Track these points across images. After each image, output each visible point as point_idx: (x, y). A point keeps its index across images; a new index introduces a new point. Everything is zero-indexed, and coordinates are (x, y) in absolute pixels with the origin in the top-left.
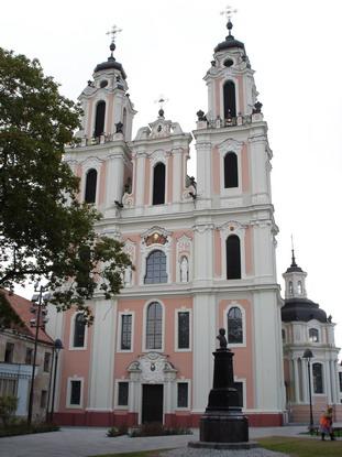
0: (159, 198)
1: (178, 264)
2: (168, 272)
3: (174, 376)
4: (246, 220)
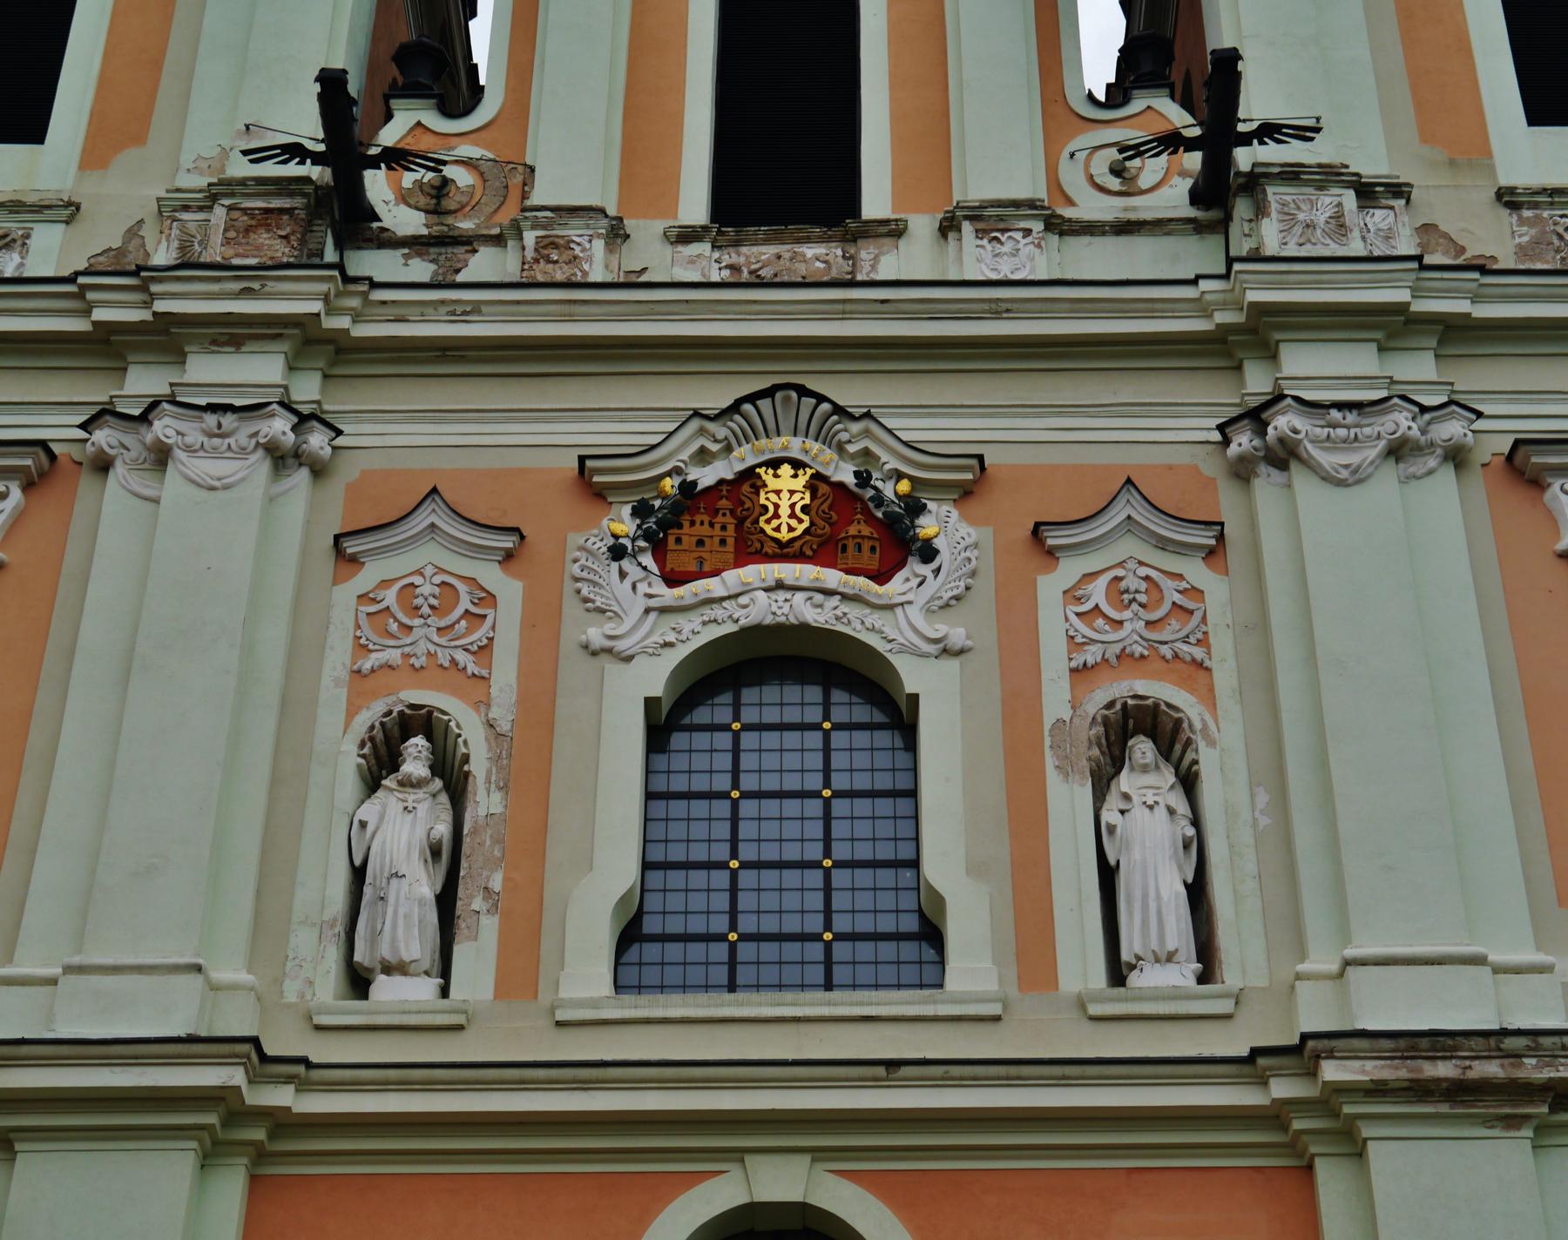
2: (945, 863)
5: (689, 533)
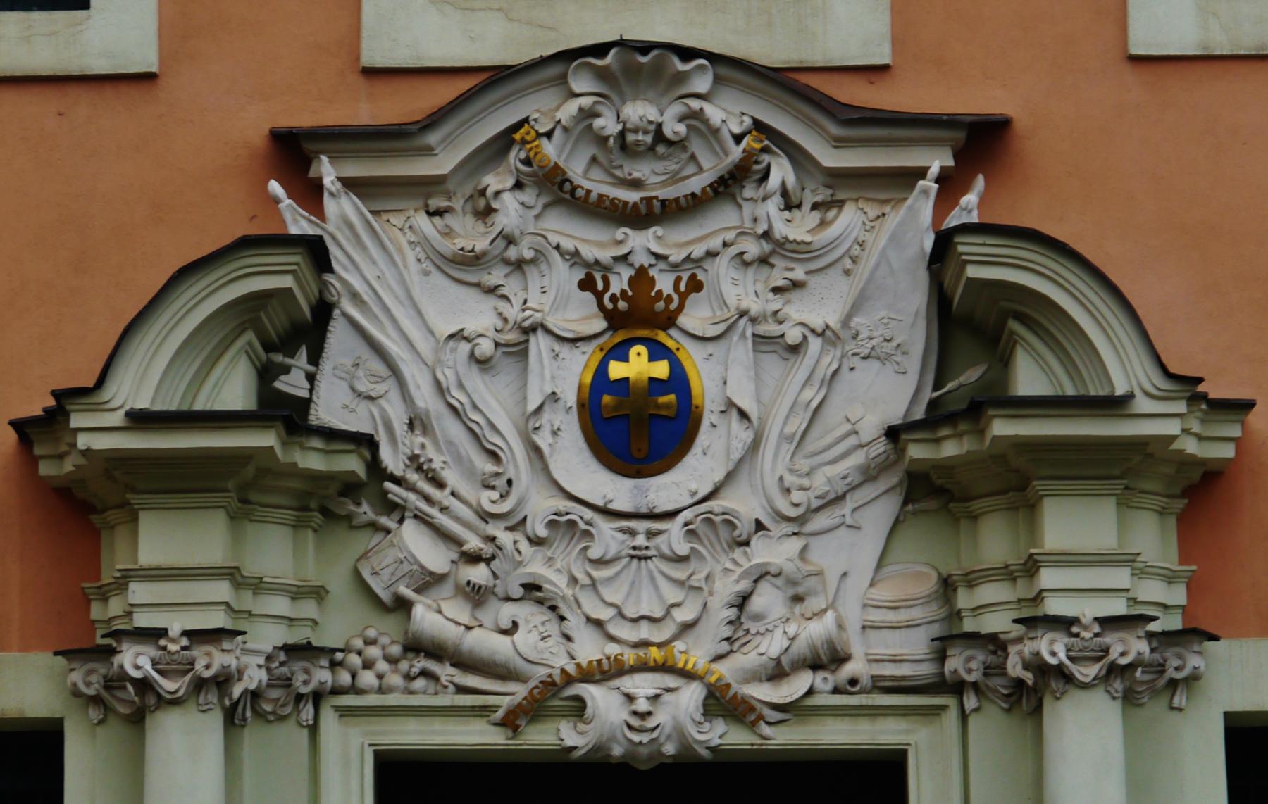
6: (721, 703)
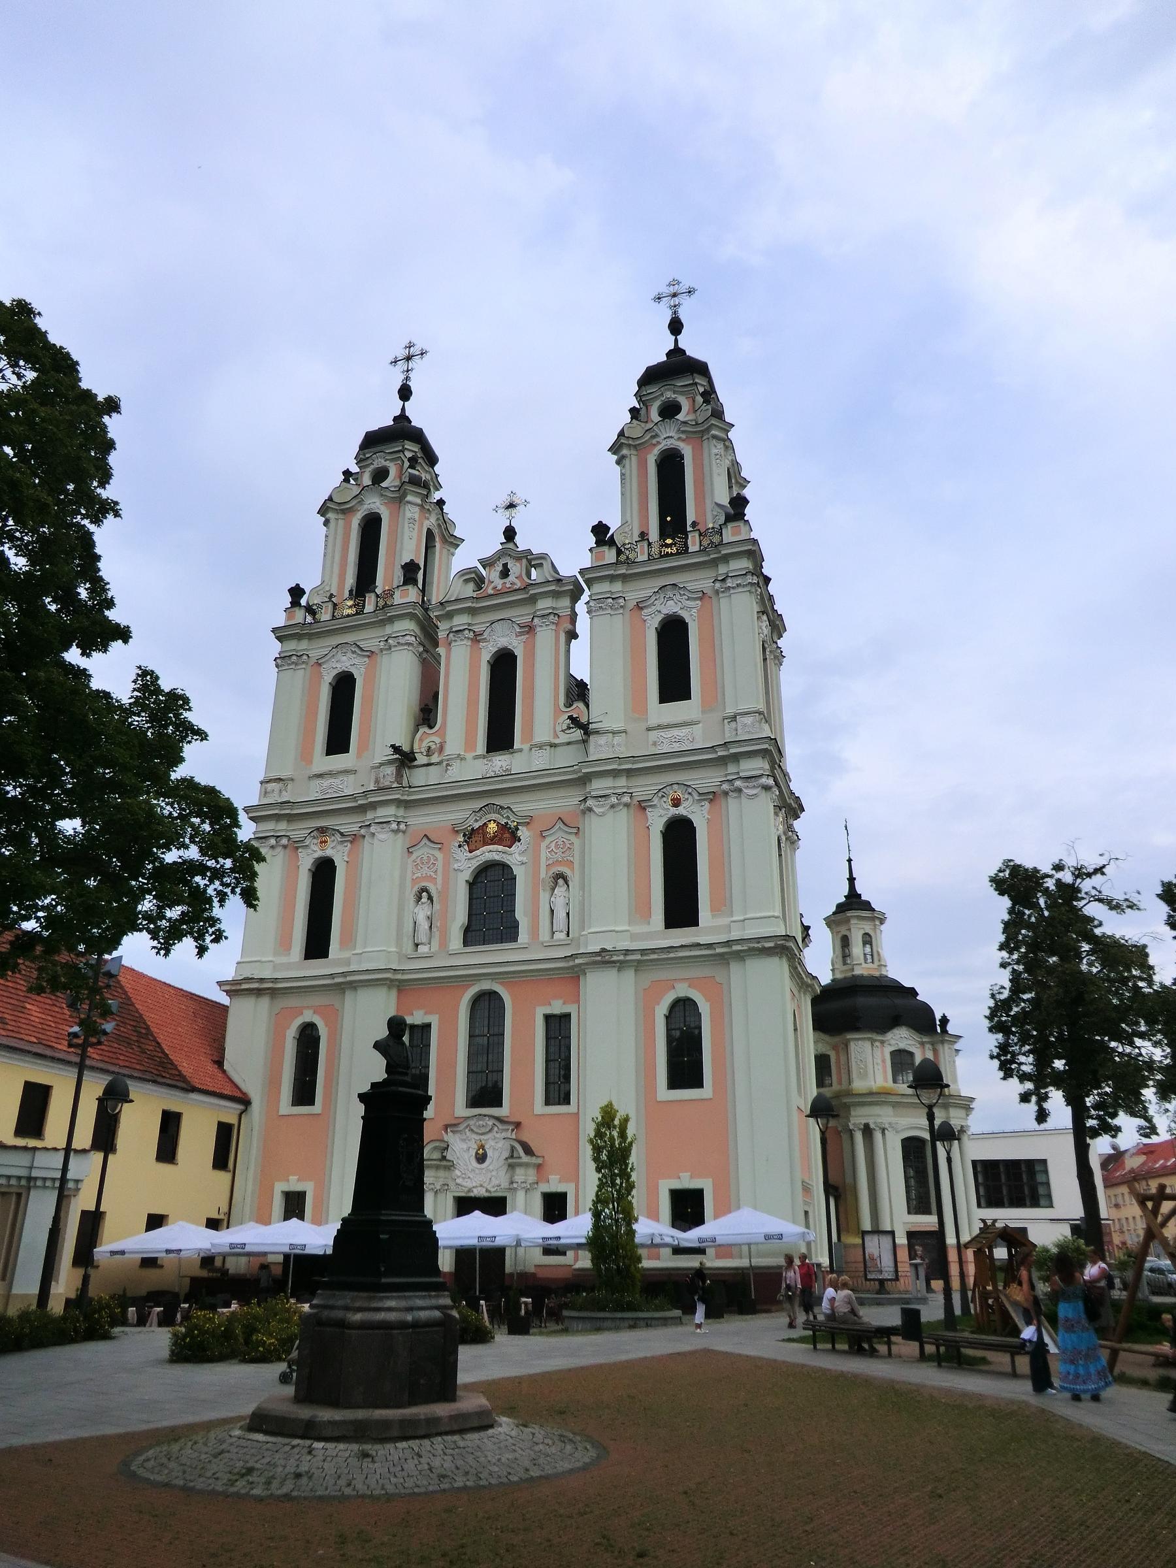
0: (500, 736)
1: (544, 896)
2: (519, 914)
3: (531, 1175)
4: (709, 779)
5: (473, 839)
6: (487, 1191)
